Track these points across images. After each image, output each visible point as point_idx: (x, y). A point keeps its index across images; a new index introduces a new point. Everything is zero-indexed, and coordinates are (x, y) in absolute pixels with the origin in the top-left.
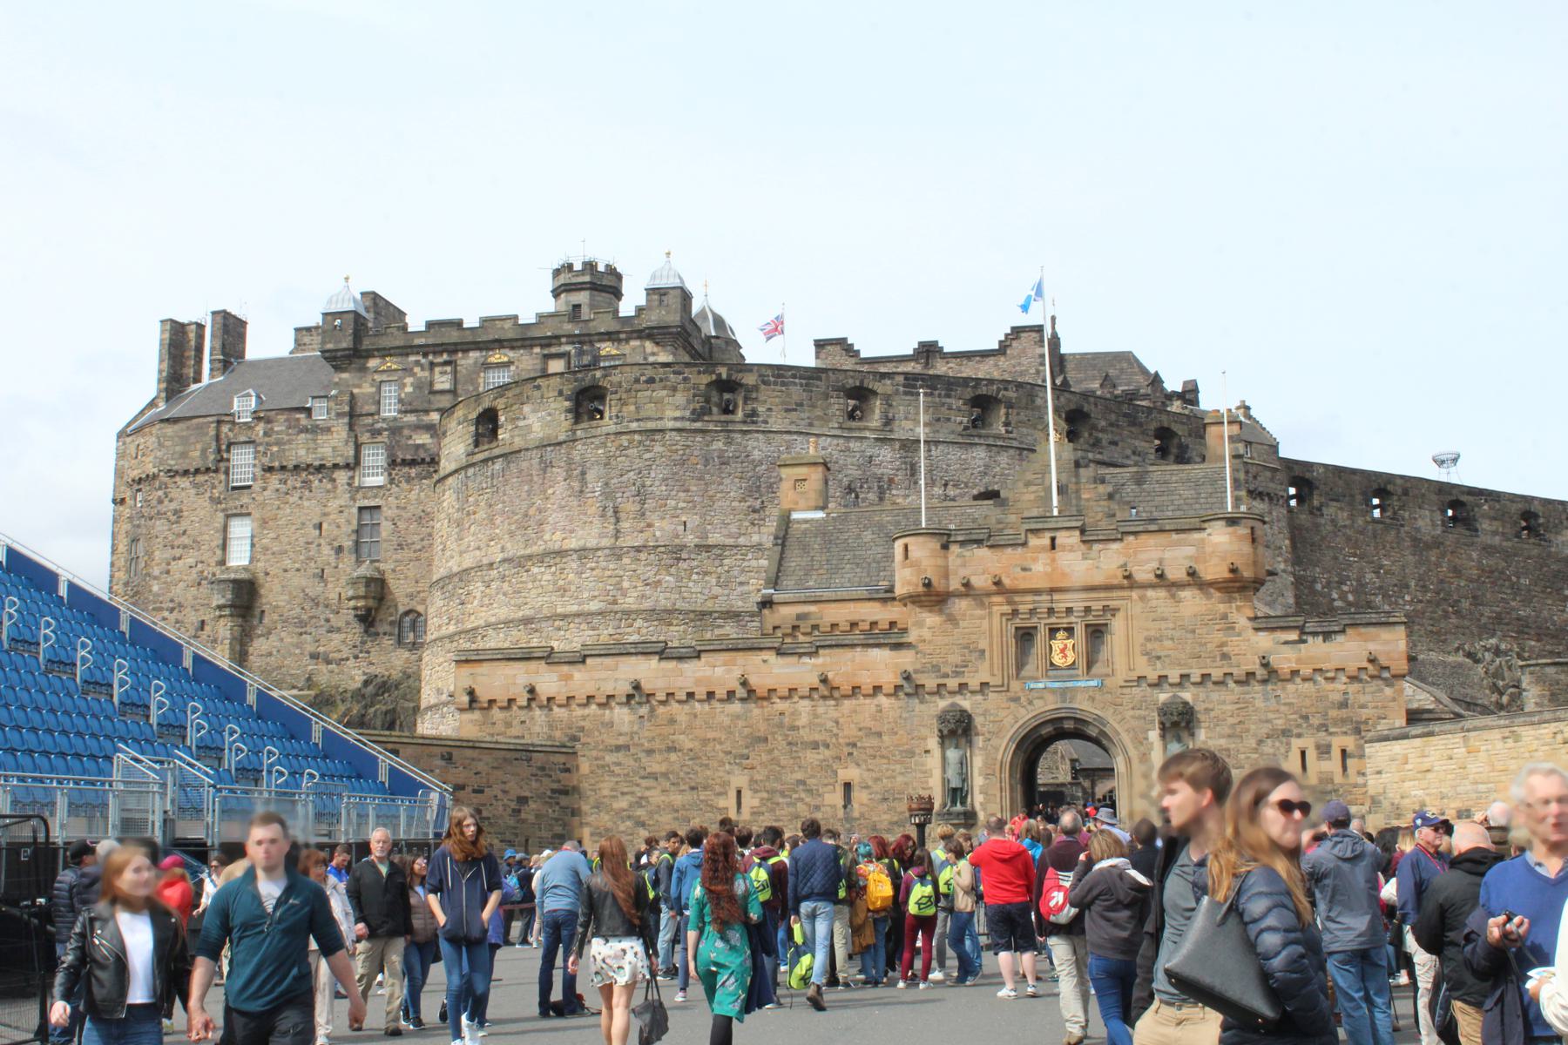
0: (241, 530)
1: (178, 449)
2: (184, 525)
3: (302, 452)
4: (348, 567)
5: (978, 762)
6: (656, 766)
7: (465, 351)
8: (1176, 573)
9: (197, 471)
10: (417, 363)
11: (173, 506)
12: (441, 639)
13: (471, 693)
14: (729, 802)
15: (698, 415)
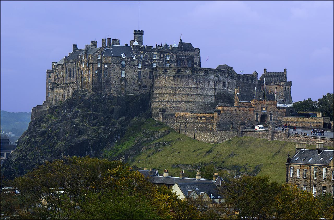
0: (123, 72)
1: (115, 60)
2: (116, 71)
3: (132, 63)
4: (137, 78)
5: (258, 117)
6: (237, 116)
7: (151, 52)
8: (272, 104)
9: (118, 64)
10: (146, 53)
11: (114, 68)
12: (172, 94)
13: (224, 109)
14: (242, 119)
15: (204, 74)
